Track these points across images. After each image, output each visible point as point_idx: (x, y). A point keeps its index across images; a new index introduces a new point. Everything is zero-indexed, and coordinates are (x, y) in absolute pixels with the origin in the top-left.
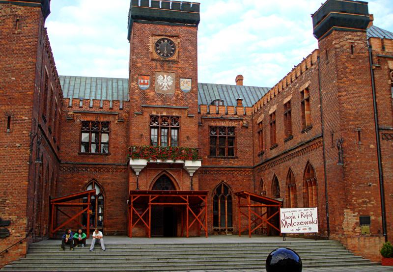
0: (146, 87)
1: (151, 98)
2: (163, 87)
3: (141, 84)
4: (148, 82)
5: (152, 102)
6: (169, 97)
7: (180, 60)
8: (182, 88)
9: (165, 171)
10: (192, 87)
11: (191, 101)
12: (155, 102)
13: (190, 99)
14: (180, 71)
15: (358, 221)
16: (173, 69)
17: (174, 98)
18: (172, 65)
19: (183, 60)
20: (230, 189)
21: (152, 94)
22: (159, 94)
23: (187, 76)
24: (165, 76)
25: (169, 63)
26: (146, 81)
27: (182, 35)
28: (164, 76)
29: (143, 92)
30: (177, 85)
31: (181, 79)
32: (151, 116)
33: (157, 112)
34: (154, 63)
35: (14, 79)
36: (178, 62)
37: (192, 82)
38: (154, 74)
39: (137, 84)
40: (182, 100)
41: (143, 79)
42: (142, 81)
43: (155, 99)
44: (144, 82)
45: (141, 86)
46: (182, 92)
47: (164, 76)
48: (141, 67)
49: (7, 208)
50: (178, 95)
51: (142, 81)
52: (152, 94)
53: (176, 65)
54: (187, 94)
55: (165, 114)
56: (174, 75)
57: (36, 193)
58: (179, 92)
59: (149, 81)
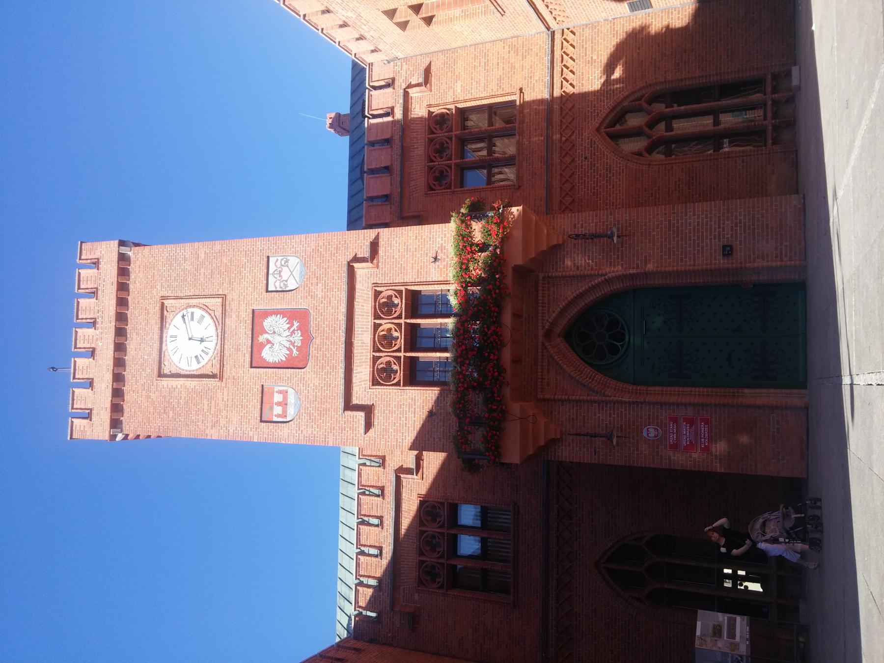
2: (293, 344)
4: (280, 392)
8: (292, 285)
9: (548, 334)
20: (626, 103)
26: (278, 398)
27: (160, 291)
32: (375, 383)
41: (272, 408)
42: (278, 410)
51: (278, 410)
53: (234, 305)
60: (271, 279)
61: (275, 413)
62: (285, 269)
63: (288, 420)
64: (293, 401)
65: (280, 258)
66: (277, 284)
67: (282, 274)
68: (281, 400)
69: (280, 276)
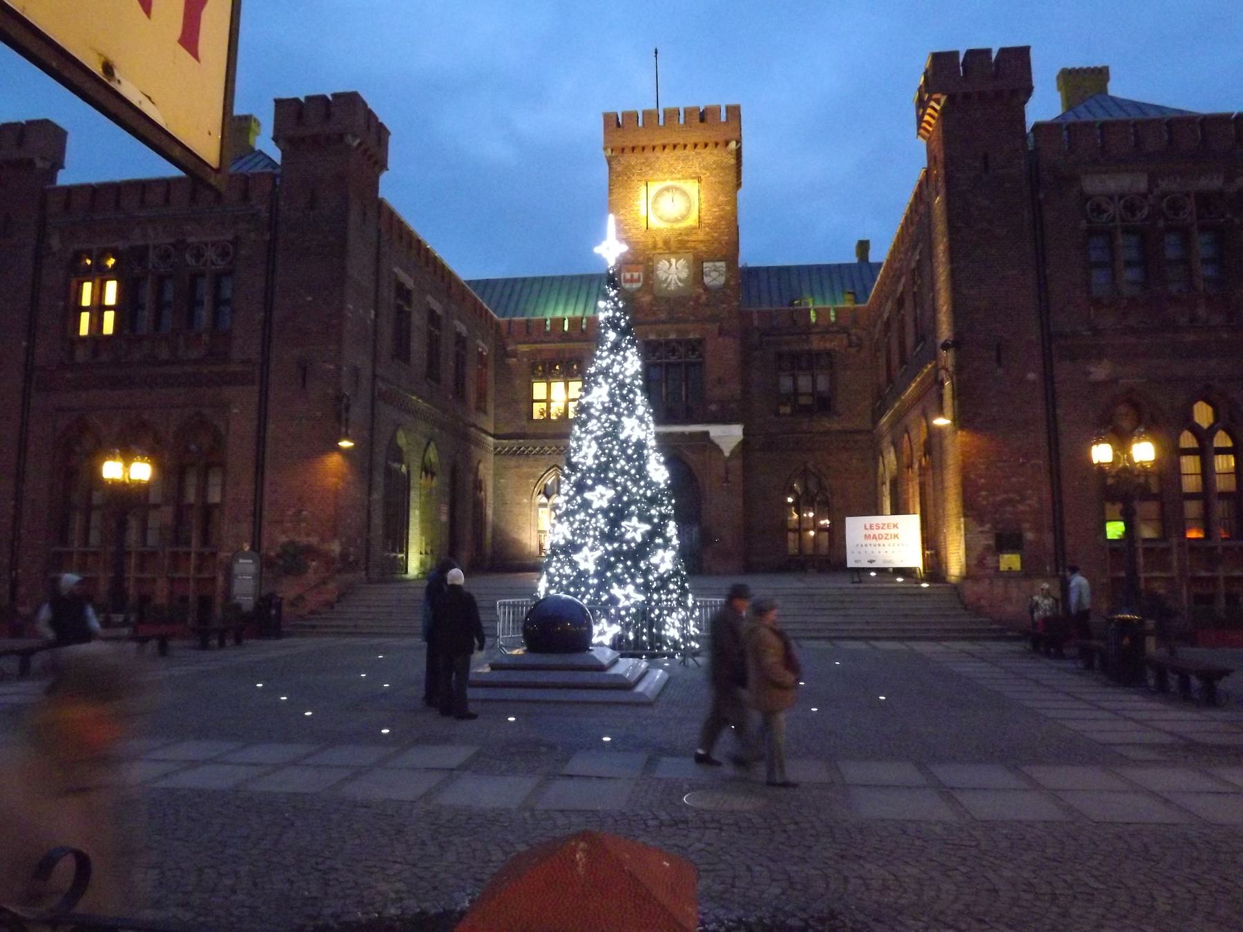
0: (636, 286)
3: (626, 281)
15: (992, 542)
24: (673, 261)
26: (636, 275)
33: (659, 335)
35: (310, 299)
41: (629, 271)
46: (706, 289)
49: (303, 525)
52: (647, 299)
55: (673, 336)
57: (377, 496)
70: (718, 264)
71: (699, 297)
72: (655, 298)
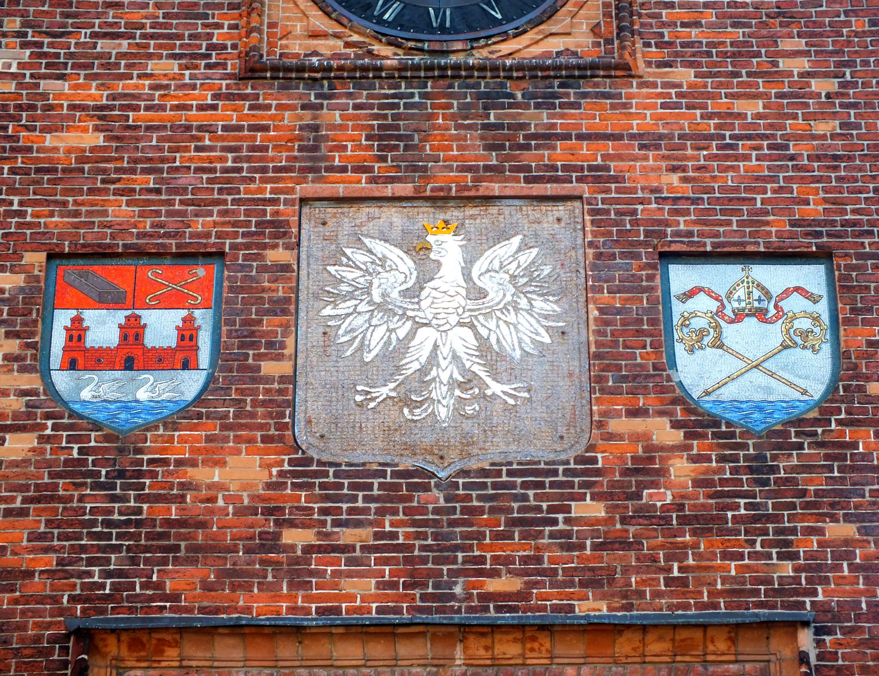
1: (224, 524)
3: (82, 356)
4: (187, 334)
5: (238, 579)
6: (511, 498)
7: (641, 57)
8: (697, 371)
10: (840, 356)
11: (839, 530)
12: (298, 573)
13: (832, 504)
14: (648, 172)
16: (531, 158)
17: (591, 509)
18: (539, 119)
19: (690, 55)
21: (243, 472)
22: (360, 475)
23: (756, 220)
24: (448, 248)
25: (491, 100)
26: (161, 326)
28: (419, 250)
29: (117, 456)
30: (628, 353)
31: (681, 277)
34: (284, 113)
36: (625, 71)
37: (840, 288)
38: (279, 230)
39: (33, 358)
40: (705, 523)
41: (108, 300)
42: (104, 328)
43: (297, 538)
44: (132, 332)
45: (90, 391)
47: (419, 250)
48: (97, 155)
50: (647, 467)
51: (104, 328)
52: (243, 472)
53: (591, 116)
54: (778, 438)
56: (562, 227)
58: (664, 432)
59: (203, 318)
60: (722, 276)
61: (90, 316)
62: (775, 334)
63: (62, 380)
64: (143, 395)
65: (823, 308)
66: (703, 304)
67: (751, 323)
68: (151, 340)
69: (739, 317)
70: (776, 277)
71: (647, 467)
72: (304, 470)
